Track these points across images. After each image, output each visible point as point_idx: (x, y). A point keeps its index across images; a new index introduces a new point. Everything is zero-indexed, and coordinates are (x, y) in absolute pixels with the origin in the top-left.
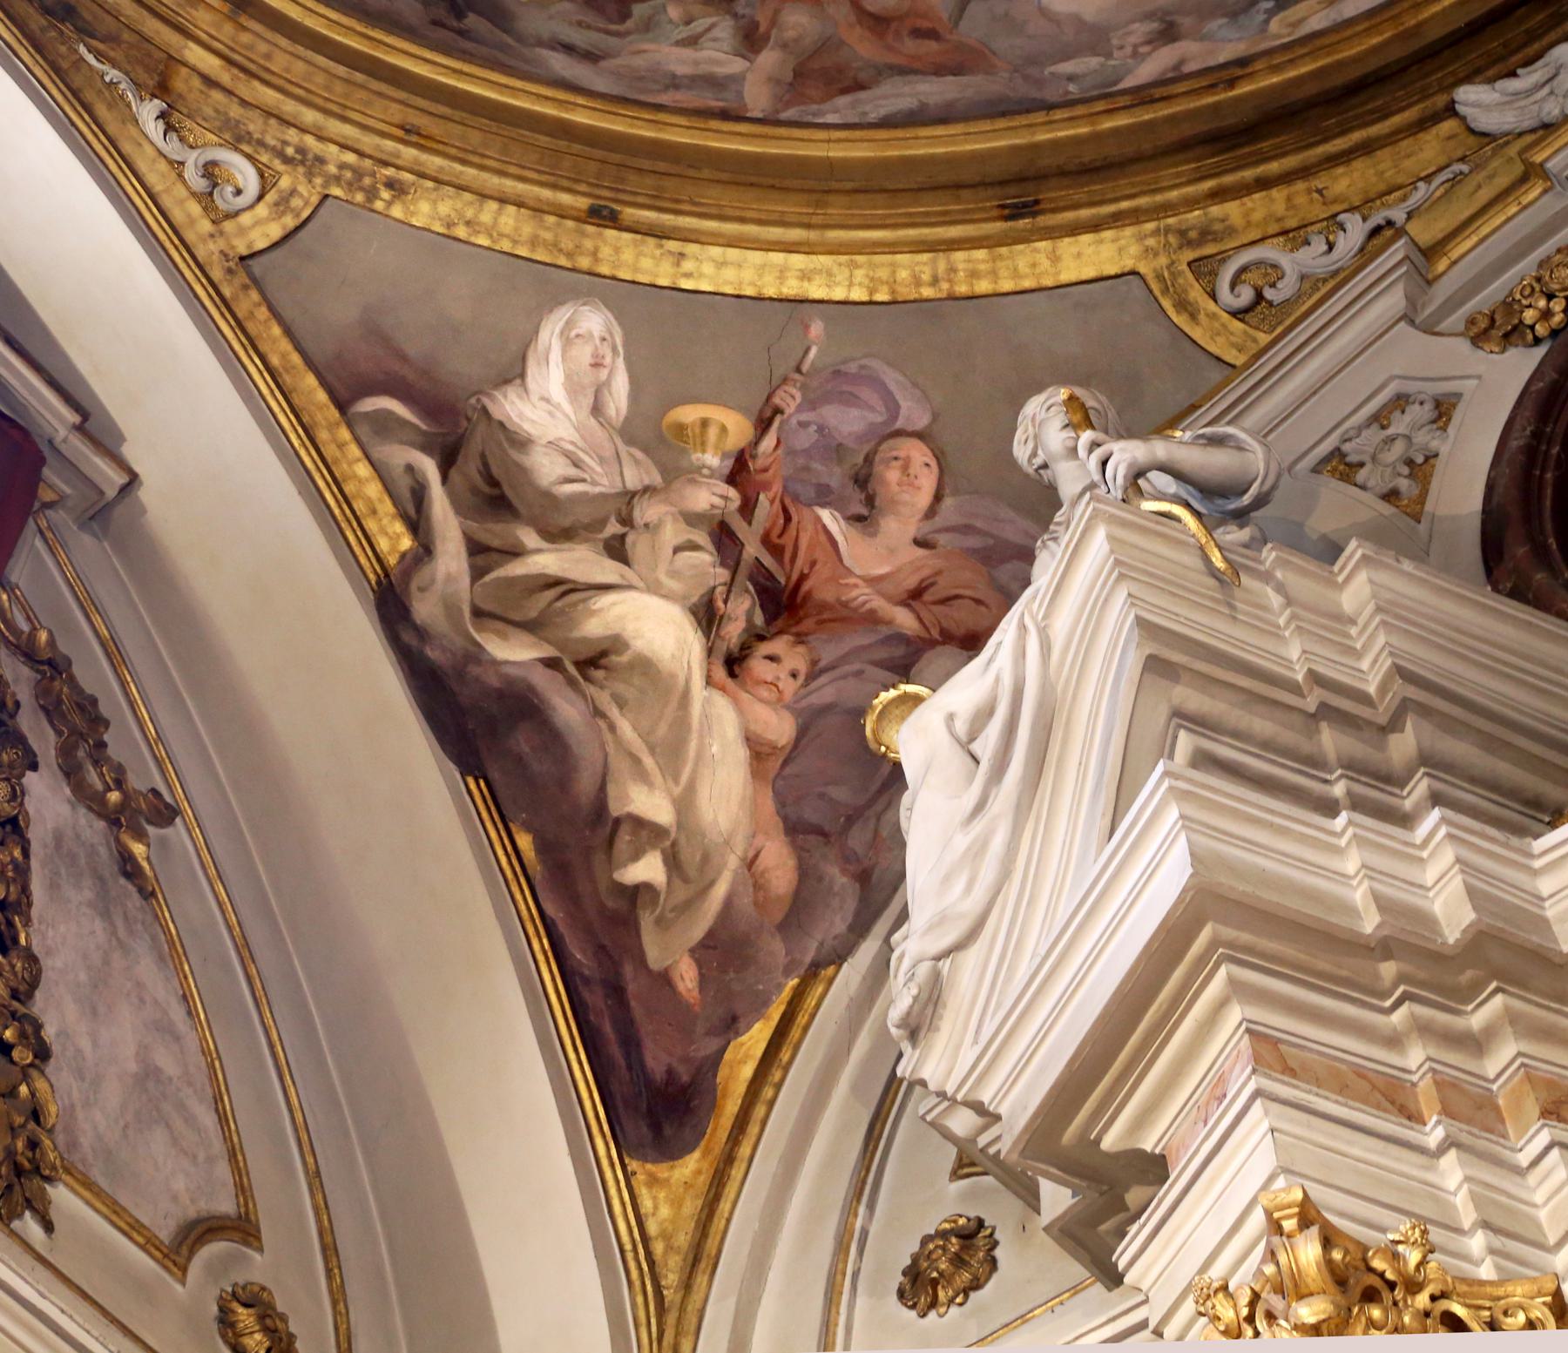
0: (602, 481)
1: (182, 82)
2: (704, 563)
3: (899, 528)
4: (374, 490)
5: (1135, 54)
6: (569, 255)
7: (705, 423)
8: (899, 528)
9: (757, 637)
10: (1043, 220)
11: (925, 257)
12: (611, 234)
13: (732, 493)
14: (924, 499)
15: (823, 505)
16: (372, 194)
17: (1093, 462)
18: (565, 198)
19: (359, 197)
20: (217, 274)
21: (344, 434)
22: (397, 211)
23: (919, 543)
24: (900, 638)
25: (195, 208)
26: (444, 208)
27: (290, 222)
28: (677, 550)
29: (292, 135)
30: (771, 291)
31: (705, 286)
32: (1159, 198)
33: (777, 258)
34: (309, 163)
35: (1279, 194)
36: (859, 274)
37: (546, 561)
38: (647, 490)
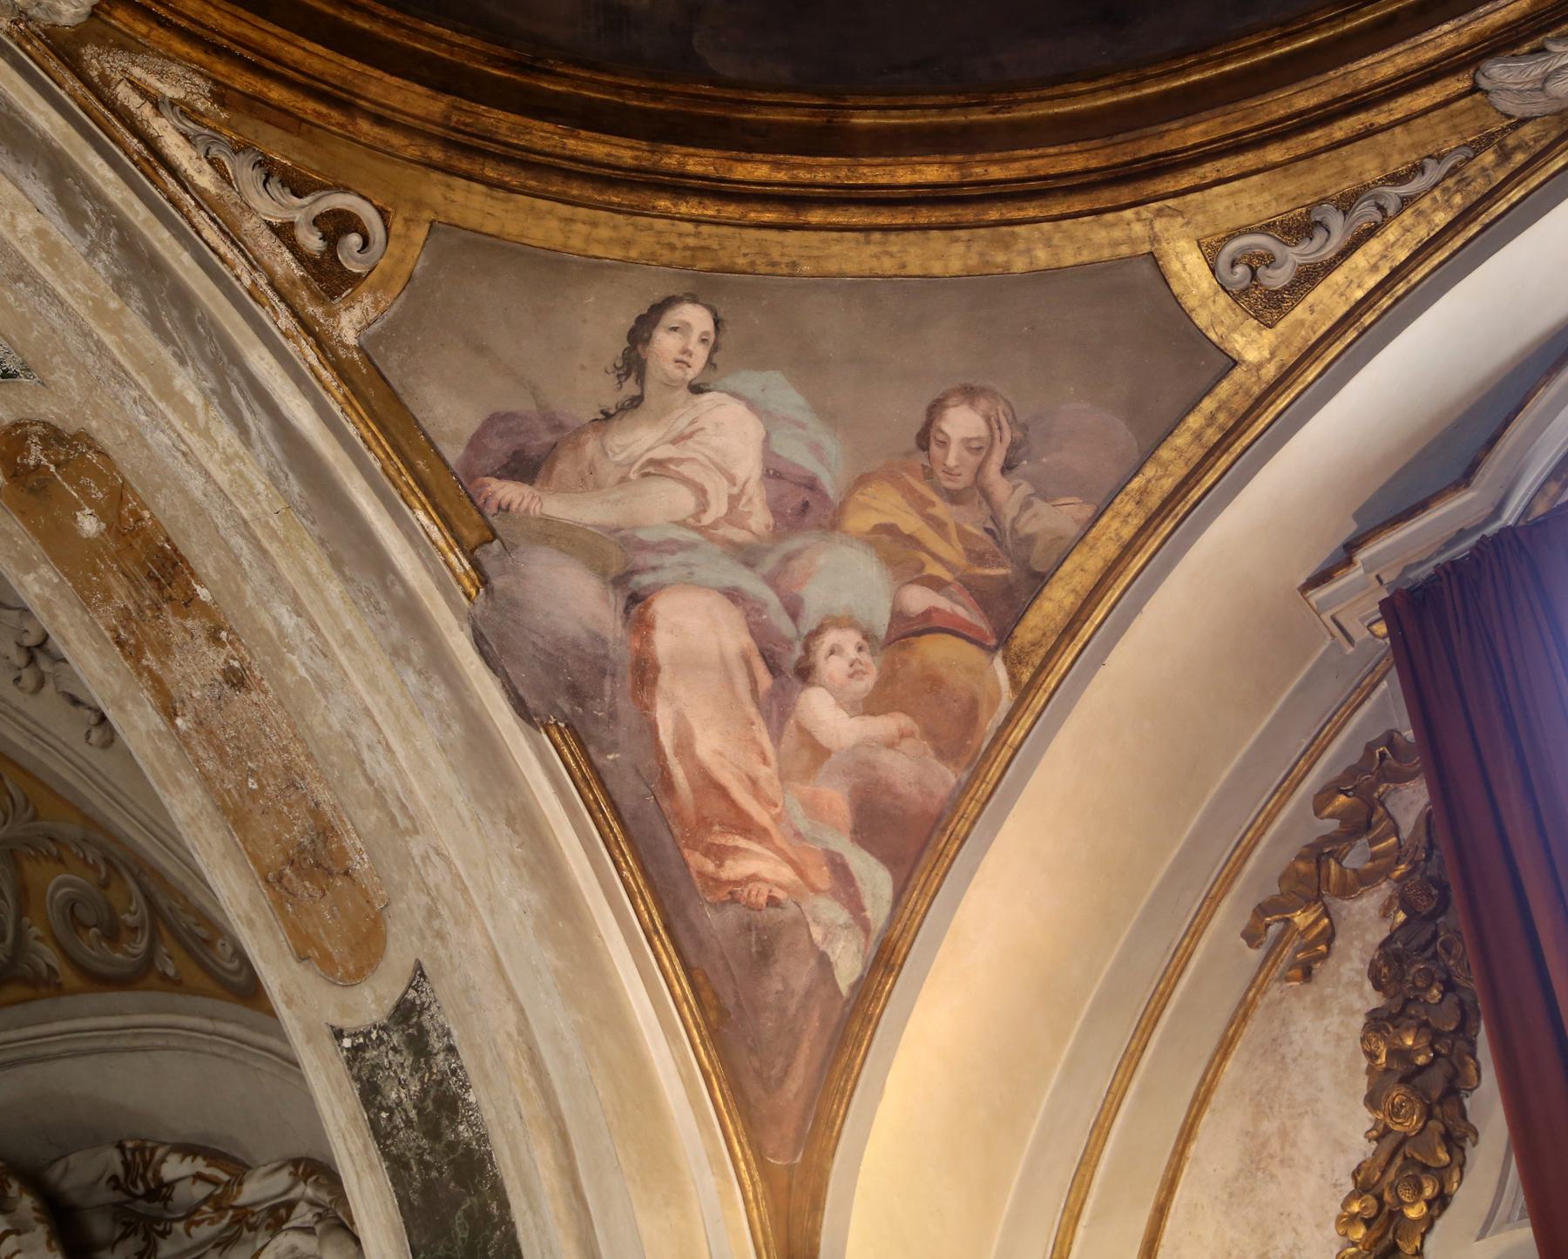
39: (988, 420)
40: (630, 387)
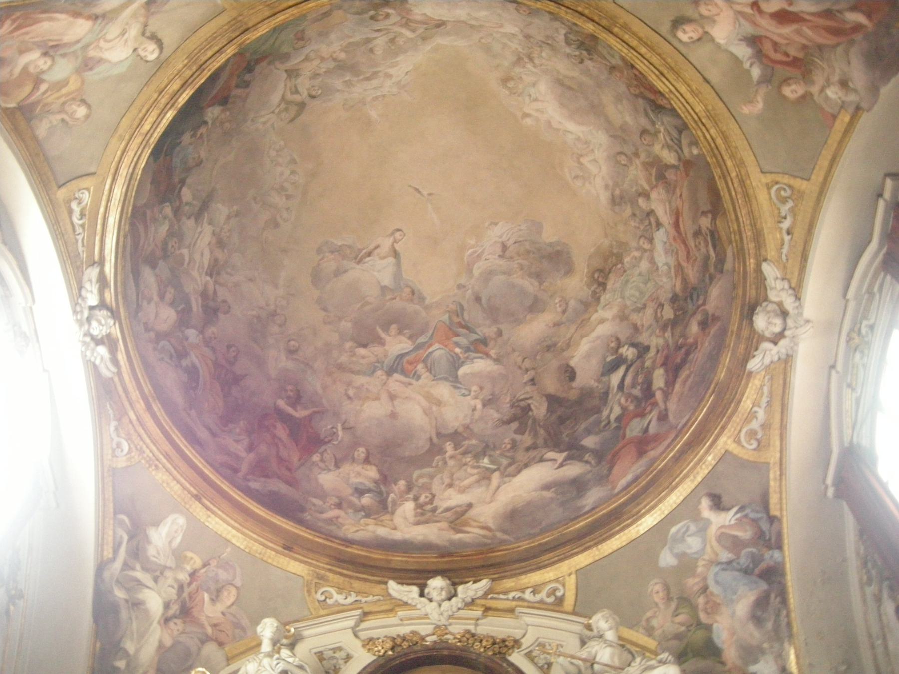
0: (162, 561)
1: (125, 420)
2: (173, 593)
3: (220, 607)
4: (110, 539)
5: (330, 507)
6: (185, 503)
7: (192, 558)
8: (220, 607)
9: (175, 616)
10: (291, 554)
11: (261, 547)
12: (197, 503)
13: (188, 578)
14: (229, 603)
15: (207, 592)
16: (150, 466)
17: (275, 662)
18: (192, 489)
19: (147, 466)
20: (106, 470)
21: (112, 522)
22: (154, 473)
23: (223, 613)
24: (206, 634)
25: (110, 452)
26: (165, 478)
27: (129, 464)
28: (169, 586)
29: (141, 443)
30: (224, 535)
31: (210, 527)
32: (318, 564)
33: (230, 528)
34: (141, 452)
35: (342, 578)
36: (245, 543)
37: (139, 574)
38: (170, 568)
39: (78, 119)
40: (148, 34)
